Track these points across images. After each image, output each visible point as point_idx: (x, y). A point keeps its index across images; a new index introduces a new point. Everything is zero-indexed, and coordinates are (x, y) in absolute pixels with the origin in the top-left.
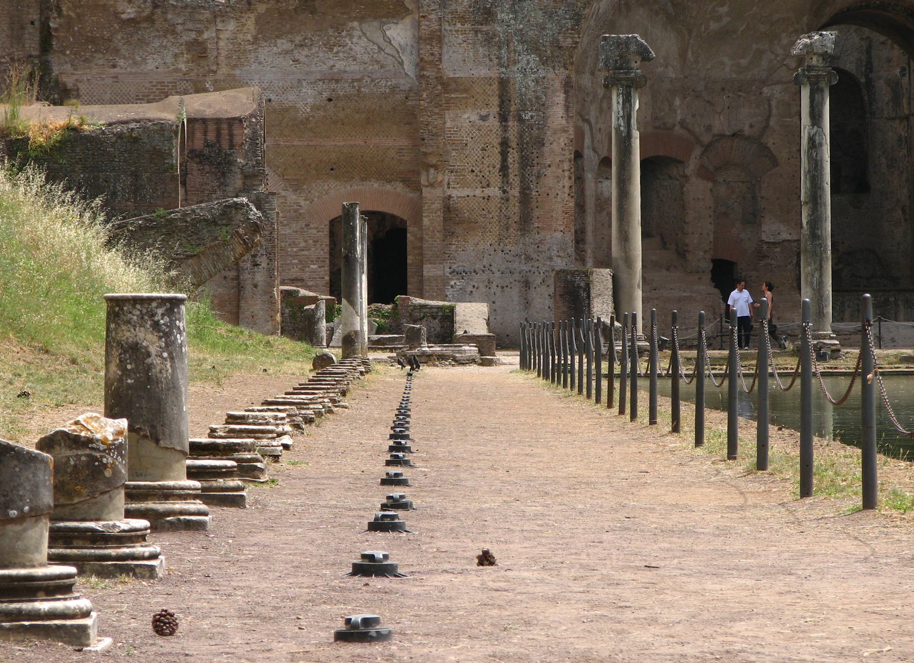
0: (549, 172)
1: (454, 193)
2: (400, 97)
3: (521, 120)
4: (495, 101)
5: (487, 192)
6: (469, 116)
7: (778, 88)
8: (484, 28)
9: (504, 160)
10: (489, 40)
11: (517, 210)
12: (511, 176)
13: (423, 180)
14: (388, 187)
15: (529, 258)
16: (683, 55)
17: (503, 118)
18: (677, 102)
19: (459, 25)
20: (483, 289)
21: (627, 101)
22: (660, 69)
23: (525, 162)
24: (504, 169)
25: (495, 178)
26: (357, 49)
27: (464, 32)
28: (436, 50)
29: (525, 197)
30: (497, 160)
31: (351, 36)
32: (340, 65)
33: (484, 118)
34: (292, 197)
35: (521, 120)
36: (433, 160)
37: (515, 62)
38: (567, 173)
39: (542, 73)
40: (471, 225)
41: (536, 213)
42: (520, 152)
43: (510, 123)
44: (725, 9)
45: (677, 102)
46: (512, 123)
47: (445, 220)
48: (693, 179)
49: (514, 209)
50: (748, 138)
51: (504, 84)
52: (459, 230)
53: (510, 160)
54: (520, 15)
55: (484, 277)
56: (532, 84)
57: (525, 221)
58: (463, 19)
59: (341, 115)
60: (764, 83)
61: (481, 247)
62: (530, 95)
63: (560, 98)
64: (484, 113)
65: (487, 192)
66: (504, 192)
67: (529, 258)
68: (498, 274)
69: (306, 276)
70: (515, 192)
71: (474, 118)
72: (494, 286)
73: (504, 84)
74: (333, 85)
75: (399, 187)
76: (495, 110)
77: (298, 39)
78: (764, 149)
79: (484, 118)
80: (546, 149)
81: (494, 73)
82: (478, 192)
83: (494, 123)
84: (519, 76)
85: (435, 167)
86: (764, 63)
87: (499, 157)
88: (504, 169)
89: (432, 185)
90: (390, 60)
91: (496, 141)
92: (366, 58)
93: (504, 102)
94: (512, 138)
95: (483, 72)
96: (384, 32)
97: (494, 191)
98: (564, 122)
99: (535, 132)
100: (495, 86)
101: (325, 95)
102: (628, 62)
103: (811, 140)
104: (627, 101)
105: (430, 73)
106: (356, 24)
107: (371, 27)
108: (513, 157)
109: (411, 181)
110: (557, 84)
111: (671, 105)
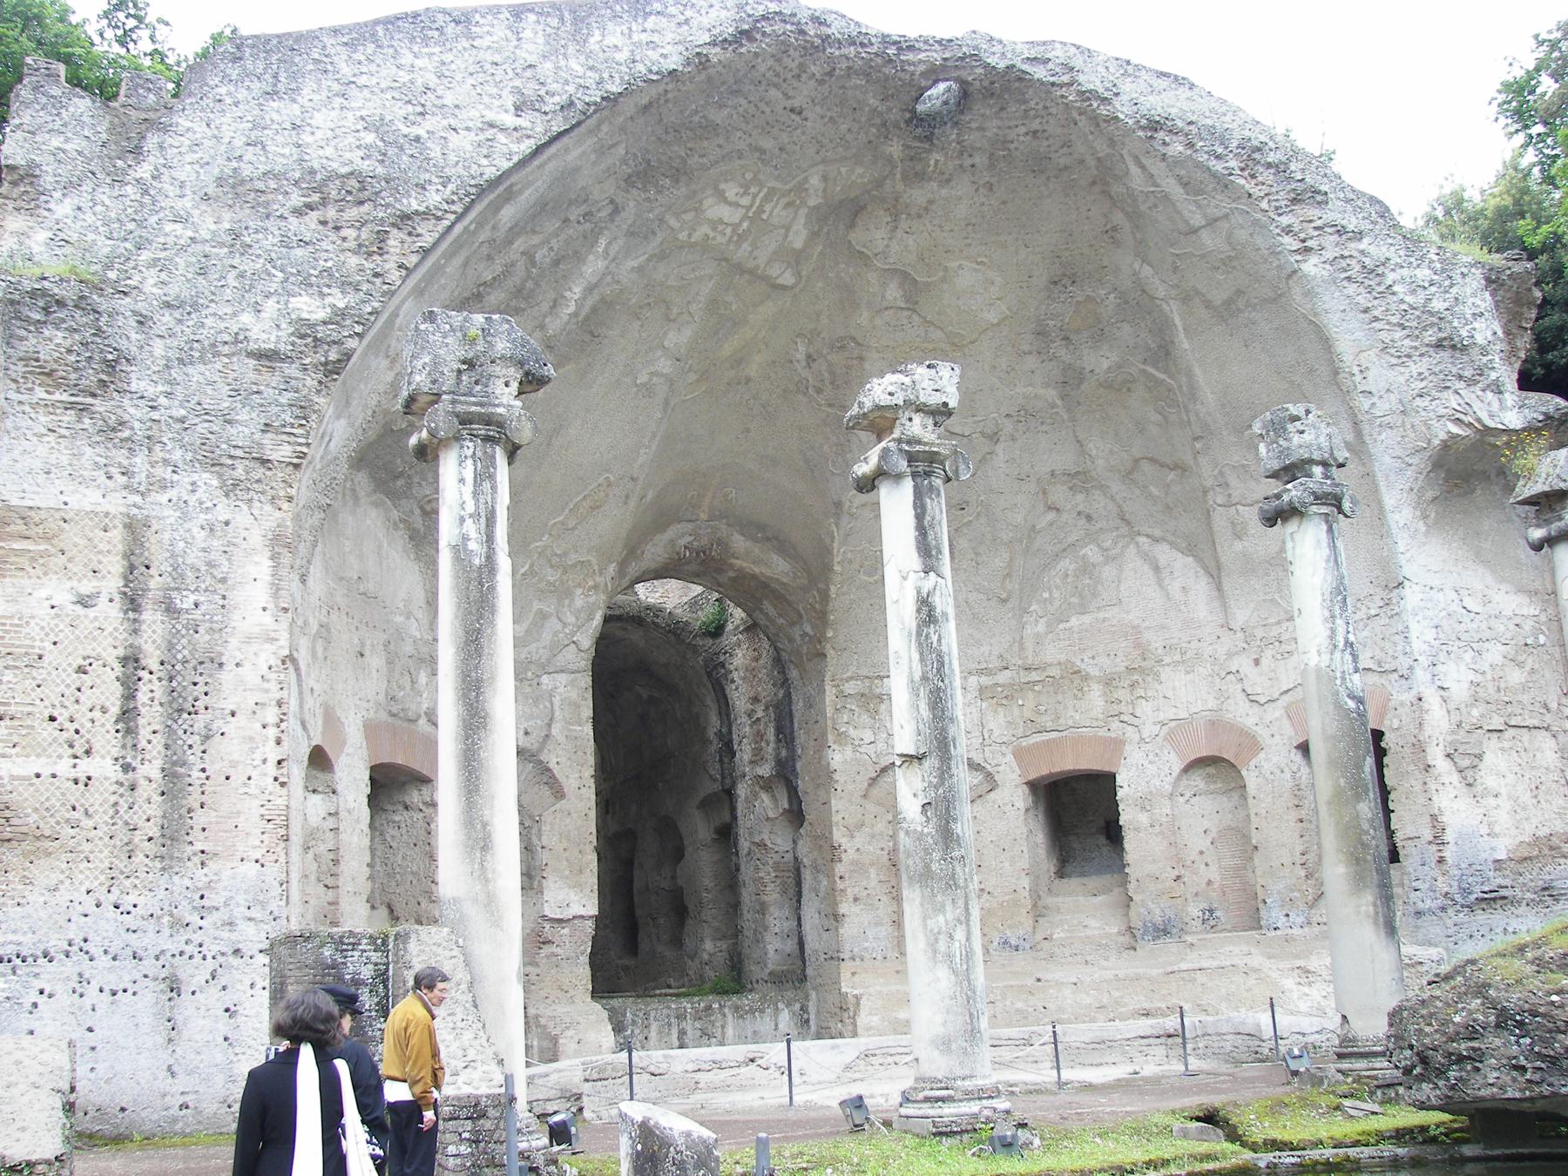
0: (231, 726)
3: (171, 610)
4: (116, 566)
5: (86, 767)
8: (99, 405)
9: (130, 695)
10: (111, 430)
11: (155, 809)
12: (144, 733)
15: (180, 925)
17: (132, 603)
19: (40, 393)
21: (485, 475)
22: (399, 619)
23: (178, 708)
24: (128, 715)
25: (107, 740)
27: (51, 407)
29: (173, 779)
30: (111, 695)
35: (171, 610)
37: (164, 486)
38: (272, 732)
39: (222, 513)
41: (200, 819)
43: (147, 616)
46: (152, 617)
51: (135, 529)
53: (142, 697)
54: (179, 391)
55: (69, 968)
56: (200, 535)
61: (63, 896)
62: (195, 557)
63: (261, 567)
64: (86, 587)
65: (86, 767)
66: (127, 768)
67: (180, 925)
68: (103, 962)
70: (151, 769)
71: (64, 597)
72: (92, 991)
73: (135, 529)
76: (112, 583)
79: (84, 602)
80: (227, 676)
81: (118, 505)
83: (110, 612)
84: (171, 515)
86: (547, 637)
87: (118, 690)
88: (128, 715)
91: (112, 655)
93: (135, 567)
94: (148, 648)
95: (86, 499)
97: (103, 767)
98: (267, 619)
99: (203, 638)
100: (117, 534)
108: (150, 691)
110: (256, 538)
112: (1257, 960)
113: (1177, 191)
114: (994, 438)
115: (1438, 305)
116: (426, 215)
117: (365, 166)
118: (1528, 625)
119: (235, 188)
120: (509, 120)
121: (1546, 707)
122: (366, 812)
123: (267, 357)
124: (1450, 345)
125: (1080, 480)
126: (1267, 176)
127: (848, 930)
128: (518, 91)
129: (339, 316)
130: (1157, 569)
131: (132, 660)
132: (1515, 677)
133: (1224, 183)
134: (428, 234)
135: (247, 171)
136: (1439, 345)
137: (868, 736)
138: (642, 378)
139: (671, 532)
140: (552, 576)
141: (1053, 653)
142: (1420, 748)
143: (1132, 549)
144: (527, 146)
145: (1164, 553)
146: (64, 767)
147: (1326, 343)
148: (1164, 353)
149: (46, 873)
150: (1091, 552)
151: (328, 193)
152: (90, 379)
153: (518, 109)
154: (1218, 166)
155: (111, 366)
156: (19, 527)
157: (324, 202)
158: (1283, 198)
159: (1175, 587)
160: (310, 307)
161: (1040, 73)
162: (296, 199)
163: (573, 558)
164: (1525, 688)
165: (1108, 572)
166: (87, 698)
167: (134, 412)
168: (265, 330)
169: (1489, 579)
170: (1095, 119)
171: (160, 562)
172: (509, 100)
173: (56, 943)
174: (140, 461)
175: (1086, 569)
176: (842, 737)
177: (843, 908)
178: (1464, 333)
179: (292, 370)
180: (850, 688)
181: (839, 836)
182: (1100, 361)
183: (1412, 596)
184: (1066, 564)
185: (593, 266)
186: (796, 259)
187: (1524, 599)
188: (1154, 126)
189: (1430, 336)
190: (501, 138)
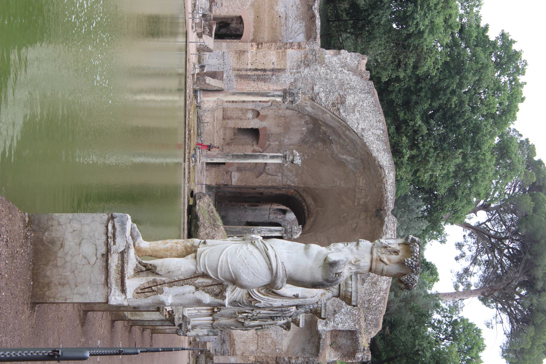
1: (249, 54)
2: (280, 39)
3: (273, 75)
4: (279, 67)
6: (274, 59)
7: (281, 179)
10: (299, 66)
13: (253, 43)
14: (251, 34)
16: (292, 145)
17: (273, 70)
18: (277, 143)
20: (218, 62)
22: (287, 137)
24: (256, 70)
25: (253, 67)
28: (295, 47)
31: (300, 23)
32: (291, 20)
33: (273, 63)
34: (249, 4)
36: (260, 46)
40: (239, 58)
42: (262, 74)
44: (306, 157)
45: (277, 143)
47: (240, 51)
48: (252, 148)
49: (244, 73)
50: (265, 168)
52: (237, 55)
55: (222, 62)
56: (284, 79)
57: (241, 77)
58: (306, 57)
59: (275, 20)
60: (282, 174)
61: (231, 62)
62: (280, 79)
64: (275, 64)
69: (223, 7)
71: (273, 61)
74: (284, 18)
75: (251, 38)
76: (276, 67)
77: (299, 6)
78: (261, 174)
79: (273, 63)
80: (263, 83)
82: (249, 61)
83: (272, 67)
85: (258, 47)
86: (288, 173)
89: (252, 46)
90: (292, 35)
91: (266, 67)
92: (293, 28)
93: (279, 70)
97: (250, 67)
101: (281, 15)
102: (292, 96)
103: (265, 156)
104: (279, 96)
105: (288, 45)
106: (304, 24)
107: (303, 29)
109: (253, 41)
111: (276, 140)
115: (343, 310)
116: (340, 113)
117: (347, 103)
118: (280, 347)
120: (360, 127)
121: (263, 348)
122: (250, 127)
131: (265, 70)
132: (269, 341)
134: (337, 113)
136: (335, 311)
138: (335, 179)
139: (313, 203)
140: (300, 171)
144: (355, 130)
146: (249, 61)
149: (235, 60)
152: (306, 62)
153: (362, 129)
155: (308, 65)
156: (284, 54)
157: (341, 98)
158: (363, 277)
160: (322, 95)
161: (384, 228)
162: (341, 94)
163: (304, 176)
164: (266, 343)
166: (259, 64)
167: (302, 70)
169: (290, 338)
171: (279, 74)
172: (364, 127)
173: (225, 61)
174: (295, 71)
178: (337, 315)
179: (311, 92)
185: (349, 158)
186: (359, 204)
187: (286, 348)
189: (337, 309)
190: (356, 126)
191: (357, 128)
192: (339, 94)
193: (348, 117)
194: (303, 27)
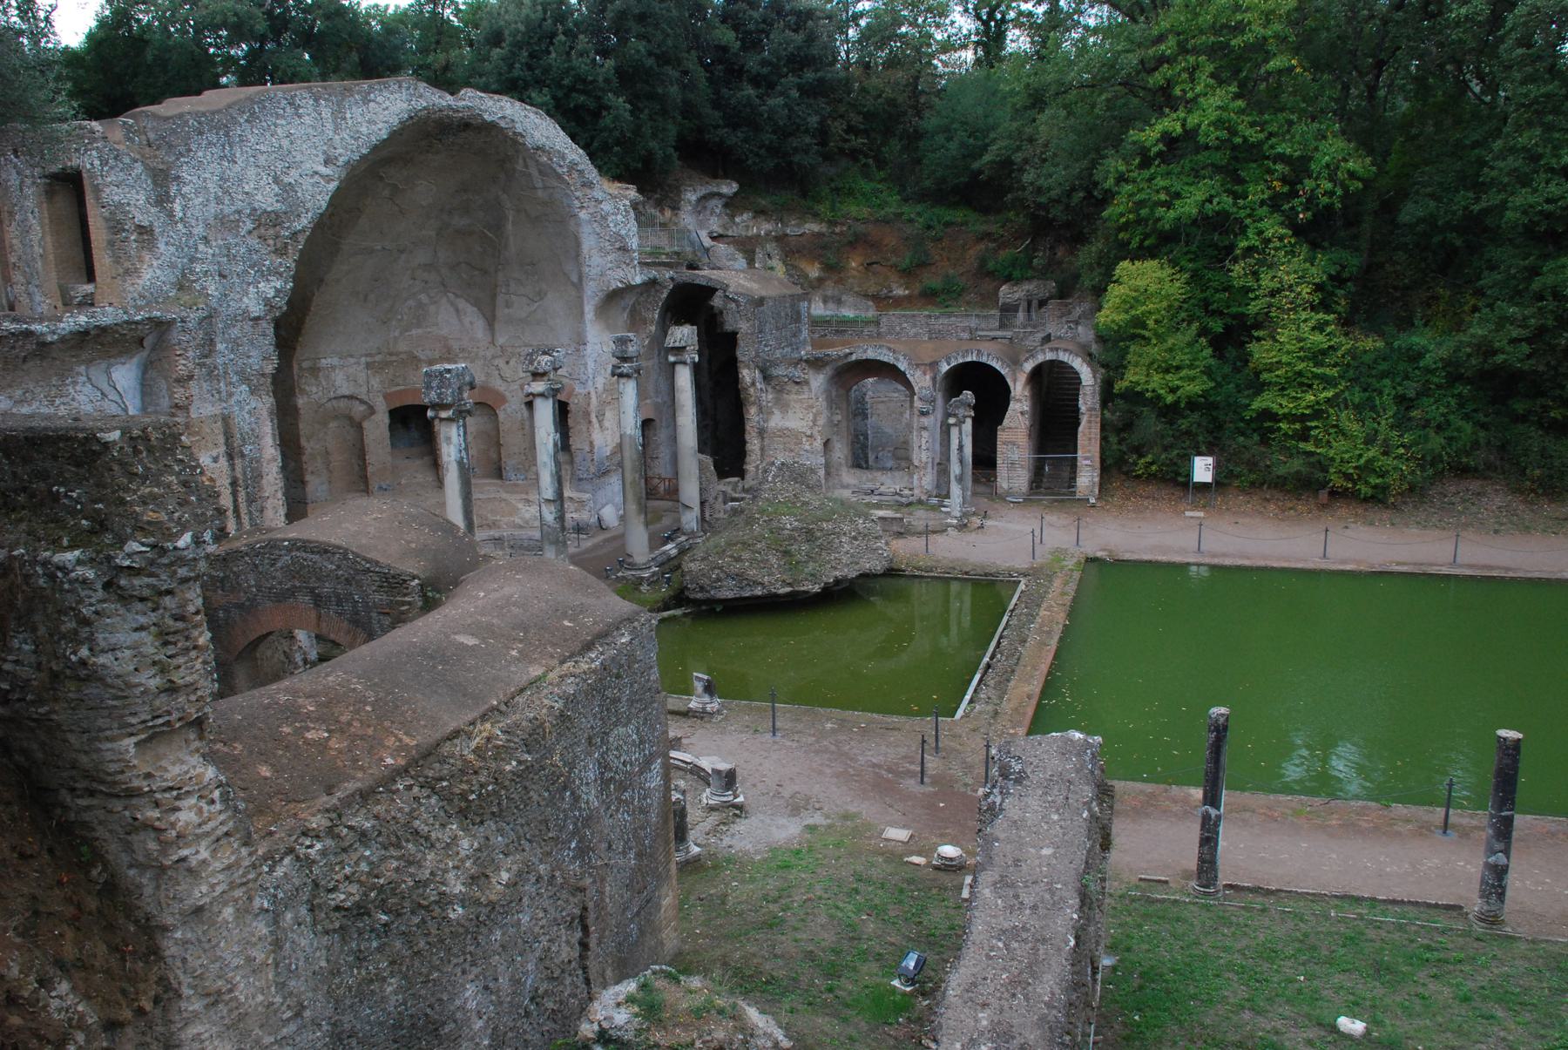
3: (243, 456)
4: (221, 439)
8: (208, 361)
17: (230, 457)
23: (251, 500)
26: (81, 398)
33: (215, 460)
37: (231, 395)
46: (238, 461)
51: (226, 419)
76: (223, 449)
80: (264, 481)
83: (223, 462)
93: (228, 436)
96: (110, 378)
107: (97, 373)
112: (504, 495)
113: (535, 173)
114: (401, 252)
115: (623, 232)
119: (225, 223)
123: (257, 319)
124: (624, 249)
125: (428, 267)
126: (575, 175)
127: (310, 488)
128: (325, 152)
129: (278, 291)
130: (457, 310)
133: (559, 177)
135: (227, 210)
137: (314, 389)
141: (402, 347)
142: (587, 414)
143: (444, 300)
144: (333, 186)
145: (462, 304)
147: (578, 244)
148: (498, 227)
150: (423, 297)
151: (267, 222)
153: (326, 163)
154: (560, 170)
159: (467, 320)
160: (269, 288)
161: (502, 124)
162: (250, 226)
165: (432, 308)
168: (256, 309)
170: (515, 142)
172: (321, 158)
175: (421, 305)
176: (303, 391)
177: (308, 478)
180: (305, 365)
181: (303, 442)
182: (459, 222)
183: (589, 348)
184: (411, 303)
188: (538, 148)
189: (617, 245)
191: (328, 179)
192: (250, 232)
193: (308, 205)
194: (93, 372)
